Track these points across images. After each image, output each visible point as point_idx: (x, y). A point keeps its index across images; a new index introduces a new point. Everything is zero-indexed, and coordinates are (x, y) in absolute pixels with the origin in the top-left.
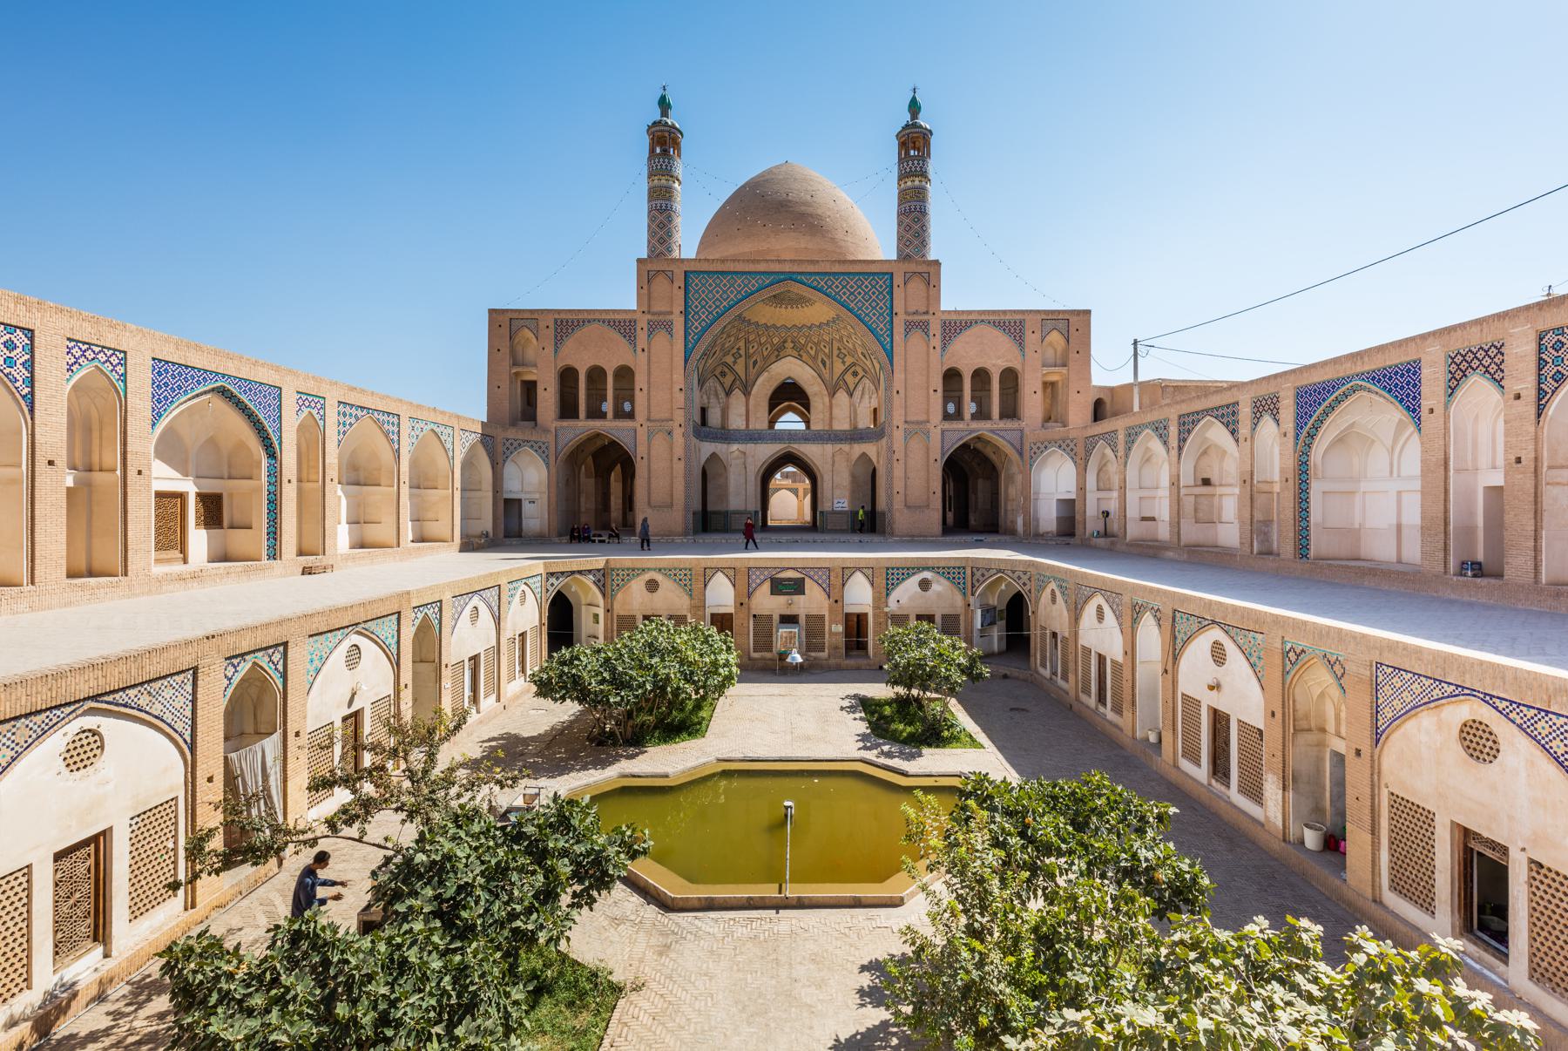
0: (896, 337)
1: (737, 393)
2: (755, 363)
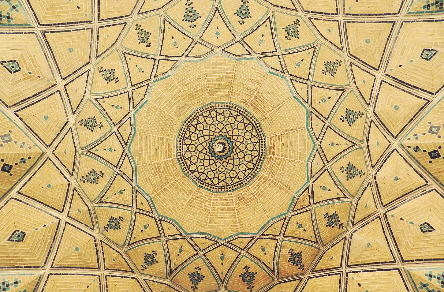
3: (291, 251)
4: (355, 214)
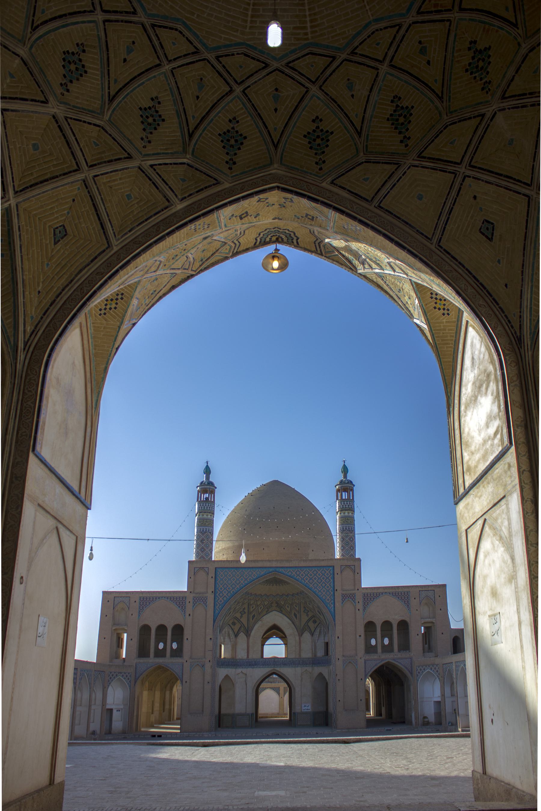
0: (337, 604)
1: (242, 635)
2: (254, 616)
3: (397, 98)
4: (514, 76)
